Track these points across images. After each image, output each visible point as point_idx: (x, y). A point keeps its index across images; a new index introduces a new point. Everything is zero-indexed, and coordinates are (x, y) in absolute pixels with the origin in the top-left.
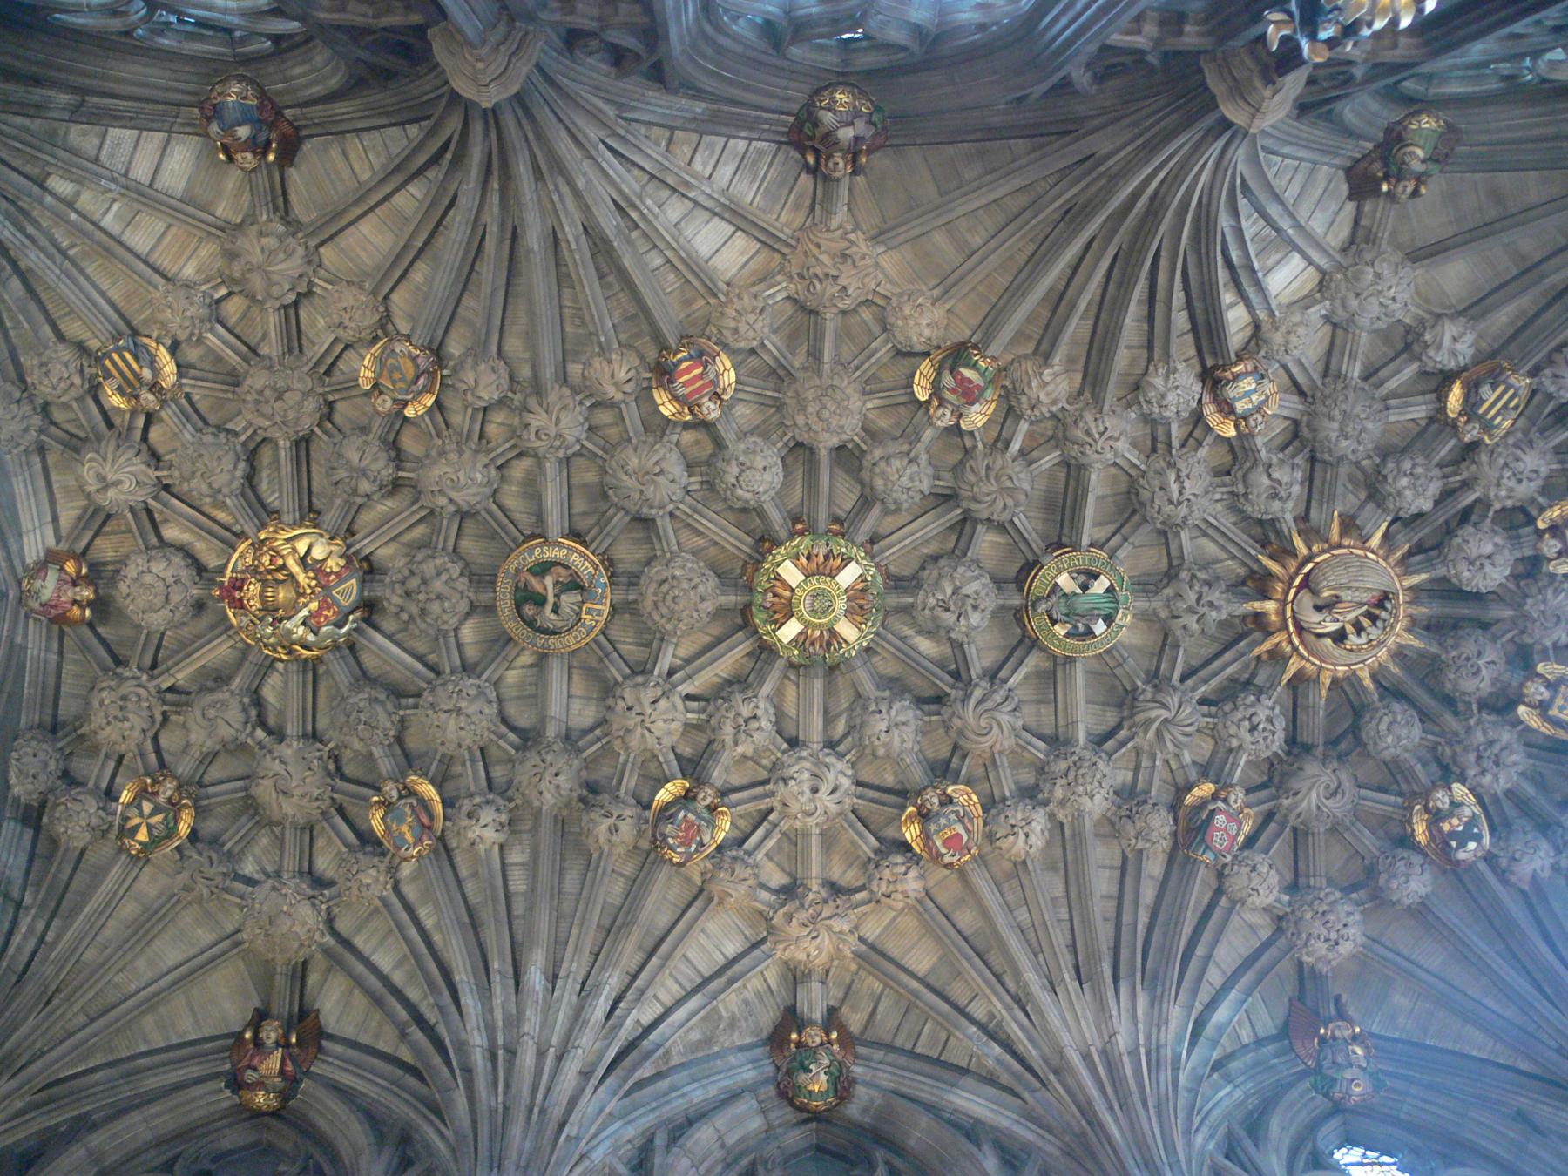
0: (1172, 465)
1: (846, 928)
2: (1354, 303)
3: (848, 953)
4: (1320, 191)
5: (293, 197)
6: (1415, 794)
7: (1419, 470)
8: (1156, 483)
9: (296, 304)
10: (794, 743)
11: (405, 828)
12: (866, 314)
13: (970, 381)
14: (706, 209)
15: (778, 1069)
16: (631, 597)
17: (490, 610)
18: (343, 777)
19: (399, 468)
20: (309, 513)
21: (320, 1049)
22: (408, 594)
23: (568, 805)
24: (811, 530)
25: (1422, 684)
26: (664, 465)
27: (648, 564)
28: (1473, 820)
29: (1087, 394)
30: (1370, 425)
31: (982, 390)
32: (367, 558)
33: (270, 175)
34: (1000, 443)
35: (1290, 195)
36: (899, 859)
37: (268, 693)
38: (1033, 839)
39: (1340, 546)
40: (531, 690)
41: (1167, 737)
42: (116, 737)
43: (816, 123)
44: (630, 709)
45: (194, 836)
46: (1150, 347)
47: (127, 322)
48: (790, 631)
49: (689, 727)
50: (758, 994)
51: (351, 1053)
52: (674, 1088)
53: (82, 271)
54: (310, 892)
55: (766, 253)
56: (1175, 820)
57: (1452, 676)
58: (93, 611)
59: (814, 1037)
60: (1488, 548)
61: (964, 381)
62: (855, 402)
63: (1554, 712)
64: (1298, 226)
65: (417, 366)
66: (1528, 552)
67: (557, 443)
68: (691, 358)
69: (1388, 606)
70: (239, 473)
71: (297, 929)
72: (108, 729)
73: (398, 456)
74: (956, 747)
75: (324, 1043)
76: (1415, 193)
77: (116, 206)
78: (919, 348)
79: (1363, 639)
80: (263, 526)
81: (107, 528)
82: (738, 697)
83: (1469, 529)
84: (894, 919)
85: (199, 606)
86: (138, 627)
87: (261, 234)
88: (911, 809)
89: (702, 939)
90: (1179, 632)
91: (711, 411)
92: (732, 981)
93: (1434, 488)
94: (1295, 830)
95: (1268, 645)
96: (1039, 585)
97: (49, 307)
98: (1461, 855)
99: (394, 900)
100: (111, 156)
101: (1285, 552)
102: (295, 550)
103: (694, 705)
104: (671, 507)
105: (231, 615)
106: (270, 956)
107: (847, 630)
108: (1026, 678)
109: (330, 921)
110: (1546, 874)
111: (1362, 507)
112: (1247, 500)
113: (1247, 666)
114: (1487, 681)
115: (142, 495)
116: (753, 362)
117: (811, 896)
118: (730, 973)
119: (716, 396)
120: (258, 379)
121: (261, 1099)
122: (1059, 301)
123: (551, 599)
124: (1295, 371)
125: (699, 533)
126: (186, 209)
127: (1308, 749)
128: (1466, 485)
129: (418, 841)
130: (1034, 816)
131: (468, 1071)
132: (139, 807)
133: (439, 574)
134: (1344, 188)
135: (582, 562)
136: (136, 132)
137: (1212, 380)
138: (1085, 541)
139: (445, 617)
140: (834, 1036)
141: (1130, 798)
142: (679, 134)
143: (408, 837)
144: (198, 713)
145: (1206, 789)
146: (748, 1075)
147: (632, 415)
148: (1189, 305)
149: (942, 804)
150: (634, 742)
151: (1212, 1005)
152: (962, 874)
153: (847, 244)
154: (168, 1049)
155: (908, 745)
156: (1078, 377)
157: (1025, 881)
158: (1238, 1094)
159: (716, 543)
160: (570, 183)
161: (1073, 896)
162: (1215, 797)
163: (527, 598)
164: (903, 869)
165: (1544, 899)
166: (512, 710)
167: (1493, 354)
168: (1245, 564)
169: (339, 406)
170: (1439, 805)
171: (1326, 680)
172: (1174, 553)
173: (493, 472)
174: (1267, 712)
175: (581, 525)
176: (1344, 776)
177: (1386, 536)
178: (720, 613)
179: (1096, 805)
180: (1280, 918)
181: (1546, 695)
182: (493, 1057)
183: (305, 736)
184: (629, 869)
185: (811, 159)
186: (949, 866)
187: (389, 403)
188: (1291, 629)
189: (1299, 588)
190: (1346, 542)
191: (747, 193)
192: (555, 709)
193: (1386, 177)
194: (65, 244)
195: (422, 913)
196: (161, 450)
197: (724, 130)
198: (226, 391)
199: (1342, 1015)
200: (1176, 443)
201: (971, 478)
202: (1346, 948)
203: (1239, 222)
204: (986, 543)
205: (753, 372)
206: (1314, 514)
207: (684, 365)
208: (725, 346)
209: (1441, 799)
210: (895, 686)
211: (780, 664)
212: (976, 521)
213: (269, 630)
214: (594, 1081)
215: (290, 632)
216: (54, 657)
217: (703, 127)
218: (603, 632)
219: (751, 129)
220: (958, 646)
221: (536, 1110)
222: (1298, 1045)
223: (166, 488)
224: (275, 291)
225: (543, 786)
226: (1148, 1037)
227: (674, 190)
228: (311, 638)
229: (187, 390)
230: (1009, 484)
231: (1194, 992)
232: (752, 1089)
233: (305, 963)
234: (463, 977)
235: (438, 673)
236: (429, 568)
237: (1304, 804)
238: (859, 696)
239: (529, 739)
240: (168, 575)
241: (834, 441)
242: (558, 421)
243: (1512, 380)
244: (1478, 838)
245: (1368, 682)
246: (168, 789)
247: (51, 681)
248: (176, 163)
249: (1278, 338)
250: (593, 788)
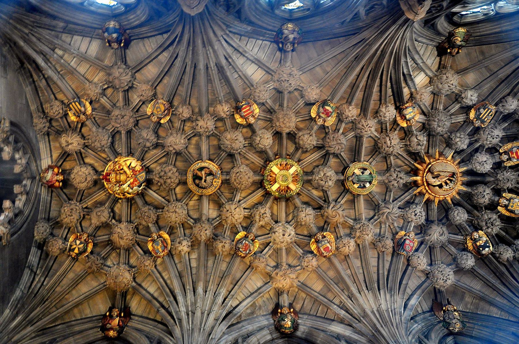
0: (388, 136)
1: (295, 277)
2: (440, 86)
3: (295, 285)
4: (429, 53)
5: (128, 59)
6: (467, 235)
7: (462, 136)
8: (383, 142)
9: (128, 90)
10: (276, 222)
11: (159, 247)
12: (296, 93)
13: (328, 110)
14: (250, 60)
15: (275, 321)
16: (228, 178)
17: (185, 183)
18: (139, 234)
19: (158, 139)
20: (130, 153)
21: (131, 318)
22: (160, 177)
23: (209, 240)
24: (281, 157)
25: (467, 201)
27: (232, 168)
28: (486, 242)
29: (362, 114)
30: (446, 123)
31: (332, 113)
32: (148, 167)
33: (121, 51)
34: (337, 130)
35: (421, 53)
36: (310, 255)
37: (116, 209)
38: (351, 248)
39: (439, 160)
40: (197, 207)
41: (390, 218)
42: (69, 221)
43: (283, 34)
44: (228, 211)
45: (92, 253)
46: (380, 100)
47: (77, 95)
48: (275, 187)
49: (245, 217)
50: (267, 298)
51: (140, 319)
52: (243, 326)
53: (64, 78)
54: (128, 269)
55: (267, 76)
56: (393, 243)
57: (476, 198)
58: (62, 183)
59: (286, 310)
60: (485, 159)
61: (326, 110)
62: (294, 119)
63: (509, 208)
64: (423, 62)
65: (165, 107)
66: (498, 160)
67: (206, 130)
69: (455, 177)
70: (109, 141)
71: (124, 280)
72: (66, 219)
73: (158, 137)
74: (326, 222)
75: (132, 316)
76: (458, 52)
77: (75, 59)
78: (313, 102)
79: (448, 187)
80: (116, 157)
81: (67, 159)
82: (260, 207)
83: (478, 154)
84: (309, 275)
85: (95, 183)
86: (76, 189)
87: (118, 68)
88: (313, 240)
89: (250, 281)
90: (391, 187)
91: (252, 120)
92: (260, 294)
93: (467, 141)
94: (430, 247)
95: (419, 190)
96: (349, 172)
97: (53, 89)
98: (484, 252)
99: (155, 270)
100: (74, 44)
101: (422, 162)
102: (126, 164)
103: (247, 210)
104: (239, 150)
105: (105, 183)
106: (116, 289)
107: (292, 186)
108: (346, 202)
109: (134, 278)
110: (512, 259)
111: (444, 149)
112: (411, 146)
113: (412, 198)
114: (487, 199)
115: (79, 148)
116: (264, 107)
117: (283, 268)
118: (259, 291)
119: (253, 116)
120: (116, 112)
121: (112, 333)
122: (354, 87)
124: (423, 108)
125: (247, 159)
127: (432, 222)
128: (476, 141)
129: (163, 251)
130: (351, 241)
131: (180, 320)
132: (76, 242)
133: (170, 171)
134: (436, 53)
135: (213, 167)
136: (81, 37)
137: (399, 109)
138: (362, 160)
139: (172, 184)
140: (292, 310)
141: (380, 237)
142: (243, 37)
143: (160, 250)
144: (95, 214)
145: (403, 233)
146: (265, 323)
147: (228, 123)
148: (392, 87)
149: (322, 238)
150: (229, 222)
151: (409, 299)
152: (329, 259)
154: (81, 319)
155: (311, 221)
156: (359, 110)
157: (349, 261)
158: (420, 326)
159: (253, 163)
160: (213, 48)
161: (364, 265)
162: (405, 235)
163: (196, 177)
164: (311, 258)
165: (512, 266)
166: (191, 213)
167: (483, 100)
168: (410, 167)
169: (140, 122)
170: (475, 237)
171: (437, 201)
172: (389, 164)
173: (187, 140)
174: (420, 210)
175: (212, 157)
176: (444, 229)
177: (452, 157)
178: (254, 183)
179: (369, 238)
180: (427, 274)
181: (507, 203)
182: (188, 315)
183: (127, 221)
184: (227, 260)
185: (281, 46)
186: (325, 257)
187: (156, 118)
188: (425, 185)
189: (427, 173)
190: (441, 158)
191: (262, 56)
192: (205, 211)
193: (449, 48)
194: (59, 70)
195: (164, 274)
196: (85, 135)
197: (255, 36)
198: (106, 117)
199: (449, 303)
200: (388, 129)
201: (328, 141)
202: (449, 282)
203: (407, 59)
204: (333, 161)
205: (264, 111)
206: (430, 151)
207: (244, 106)
208: (255, 102)
209: (476, 235)
210: (307, 203)
211: (272, 197)
212: (329, 154)
213: (118, 188)
214: (219, 322)
215: (124, 189)
216: (49, 198)
217: (250, 35)
218: (219, 189)
219: (264, 36)
220: (325, 192)
221: (202, 329)
222: (437, 313)
223: (87, 146)
224: (122, 85)
225: (202, 233)
226: (391, 306)
227: (241, 54)
228: (131, 191)
229: (94, 116)
230: (340, 142)
231: (404, 294)
232: (267, 327)
233: (126, 292)
234: (178, 291)
235: (169, 201)
236: (167, 169)
237: (433, 238)
238: (296, 207)
239: (197, 221)
240: (87, 172)
241: (287, 131)
242: (207, 124)
243: (490, 107)
244: (489, 247)
245: (450, 201)
246: (85, 236)
247: (48, 205)
249: (418, 97)
250: (216, 236)
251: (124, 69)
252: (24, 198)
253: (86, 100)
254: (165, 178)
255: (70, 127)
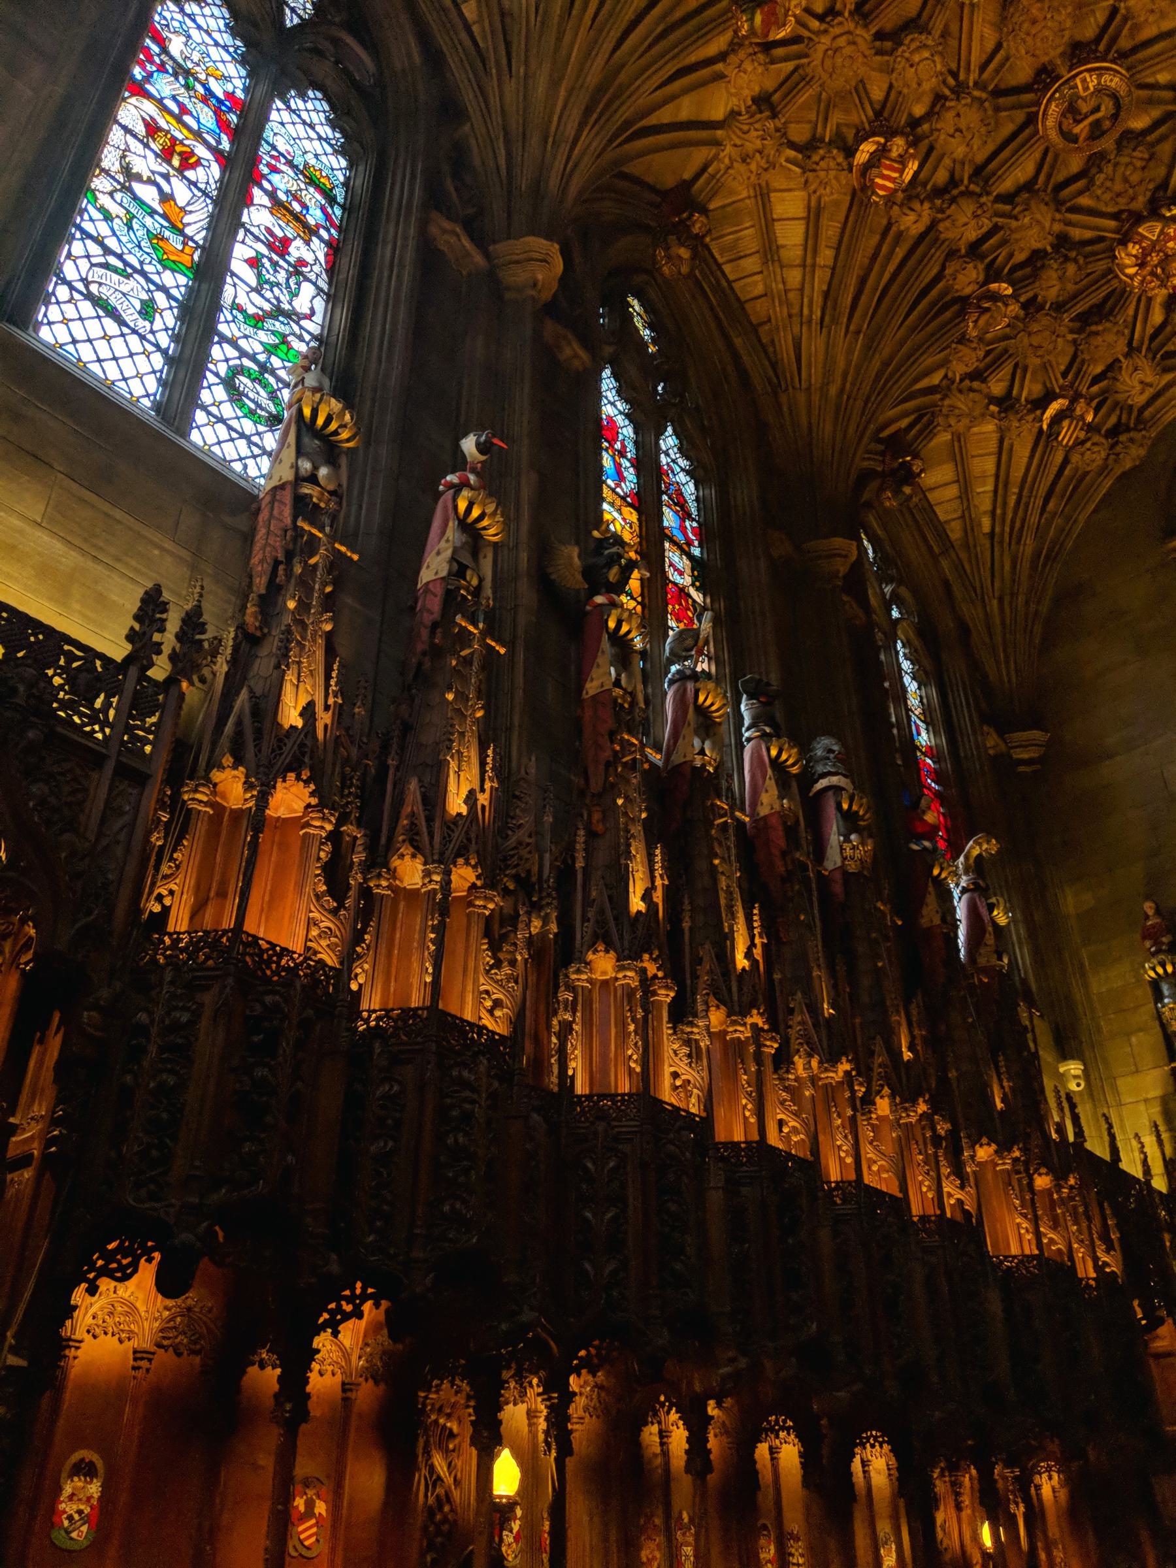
26: (951, 131)
68: (874, 193)
70: (1100, 328)
102: (1136, 273)
123: (1091, 119)
126: (958, 454)
136: (935, 508)
153: (735, 164)
173: (1018, 209)
207: (881, 193)
229: (1061, 381)
242: (966, 224)
248: (938, 478)
251: (947, 416)
253: (1041, 420)
254: (1131, 191)
255: (1105, 400)
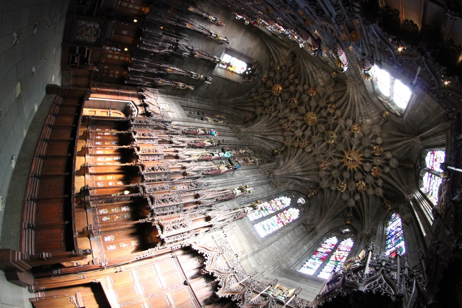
128: (372, 159)
252: (252, 80)
